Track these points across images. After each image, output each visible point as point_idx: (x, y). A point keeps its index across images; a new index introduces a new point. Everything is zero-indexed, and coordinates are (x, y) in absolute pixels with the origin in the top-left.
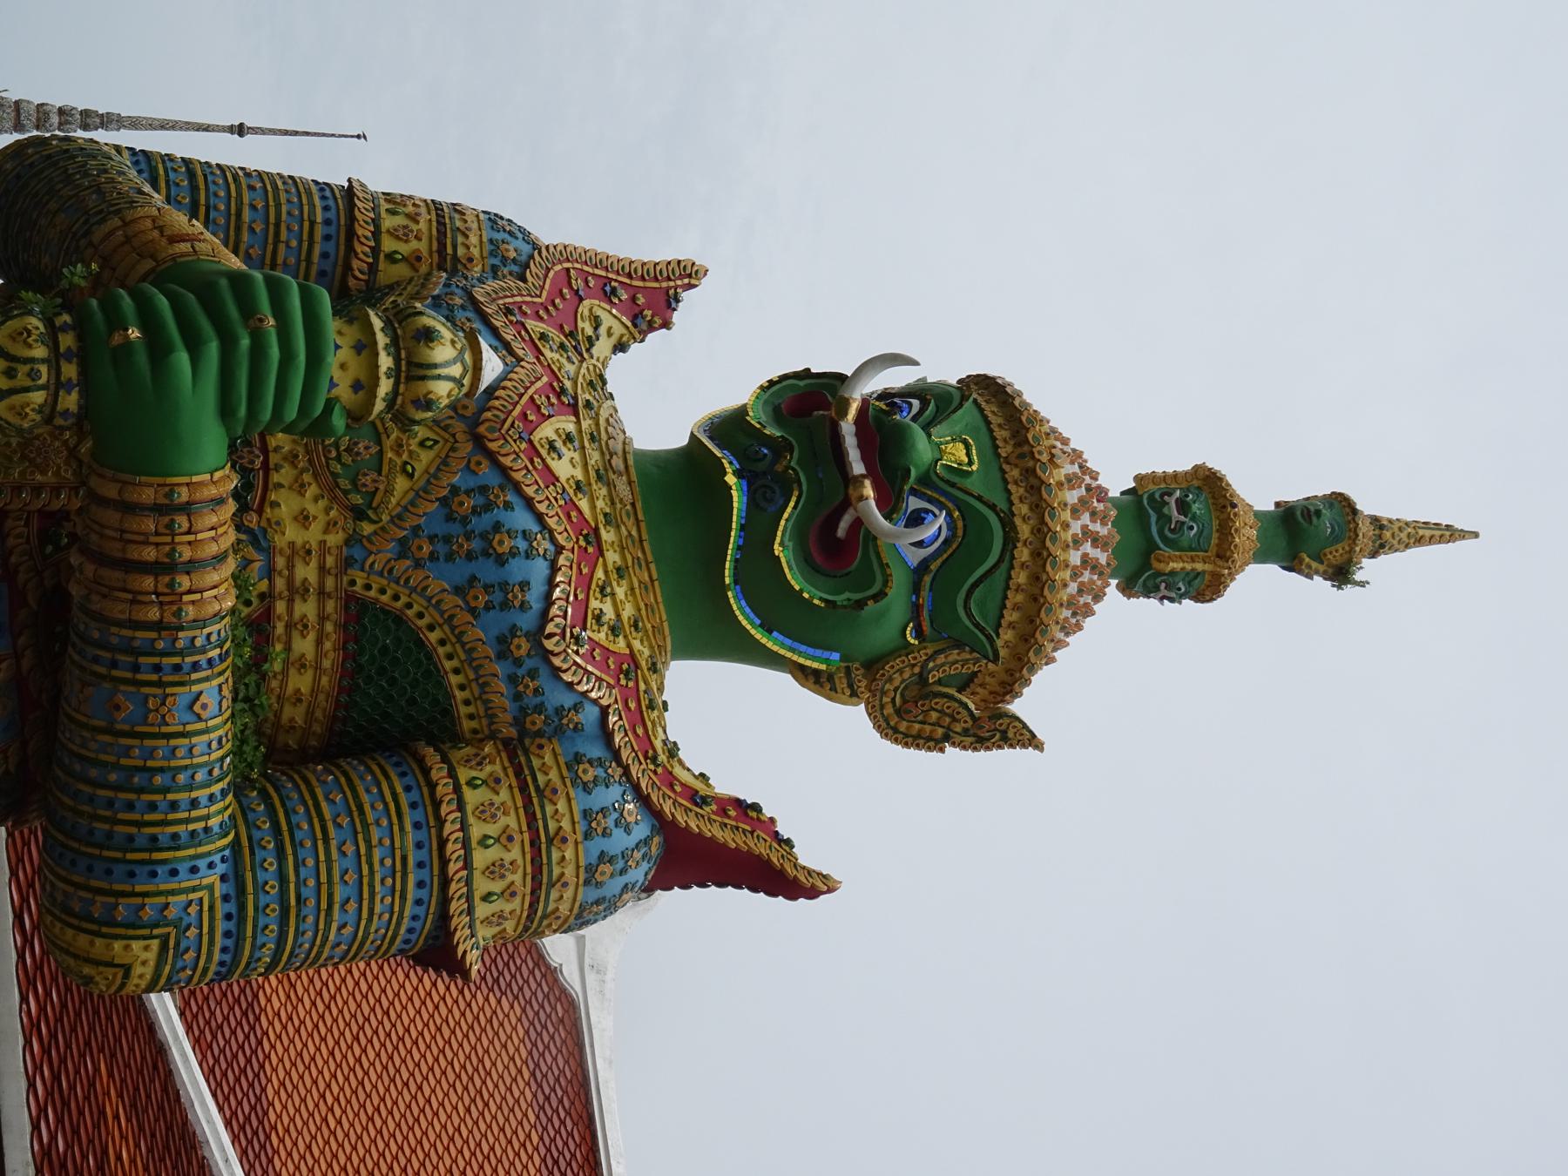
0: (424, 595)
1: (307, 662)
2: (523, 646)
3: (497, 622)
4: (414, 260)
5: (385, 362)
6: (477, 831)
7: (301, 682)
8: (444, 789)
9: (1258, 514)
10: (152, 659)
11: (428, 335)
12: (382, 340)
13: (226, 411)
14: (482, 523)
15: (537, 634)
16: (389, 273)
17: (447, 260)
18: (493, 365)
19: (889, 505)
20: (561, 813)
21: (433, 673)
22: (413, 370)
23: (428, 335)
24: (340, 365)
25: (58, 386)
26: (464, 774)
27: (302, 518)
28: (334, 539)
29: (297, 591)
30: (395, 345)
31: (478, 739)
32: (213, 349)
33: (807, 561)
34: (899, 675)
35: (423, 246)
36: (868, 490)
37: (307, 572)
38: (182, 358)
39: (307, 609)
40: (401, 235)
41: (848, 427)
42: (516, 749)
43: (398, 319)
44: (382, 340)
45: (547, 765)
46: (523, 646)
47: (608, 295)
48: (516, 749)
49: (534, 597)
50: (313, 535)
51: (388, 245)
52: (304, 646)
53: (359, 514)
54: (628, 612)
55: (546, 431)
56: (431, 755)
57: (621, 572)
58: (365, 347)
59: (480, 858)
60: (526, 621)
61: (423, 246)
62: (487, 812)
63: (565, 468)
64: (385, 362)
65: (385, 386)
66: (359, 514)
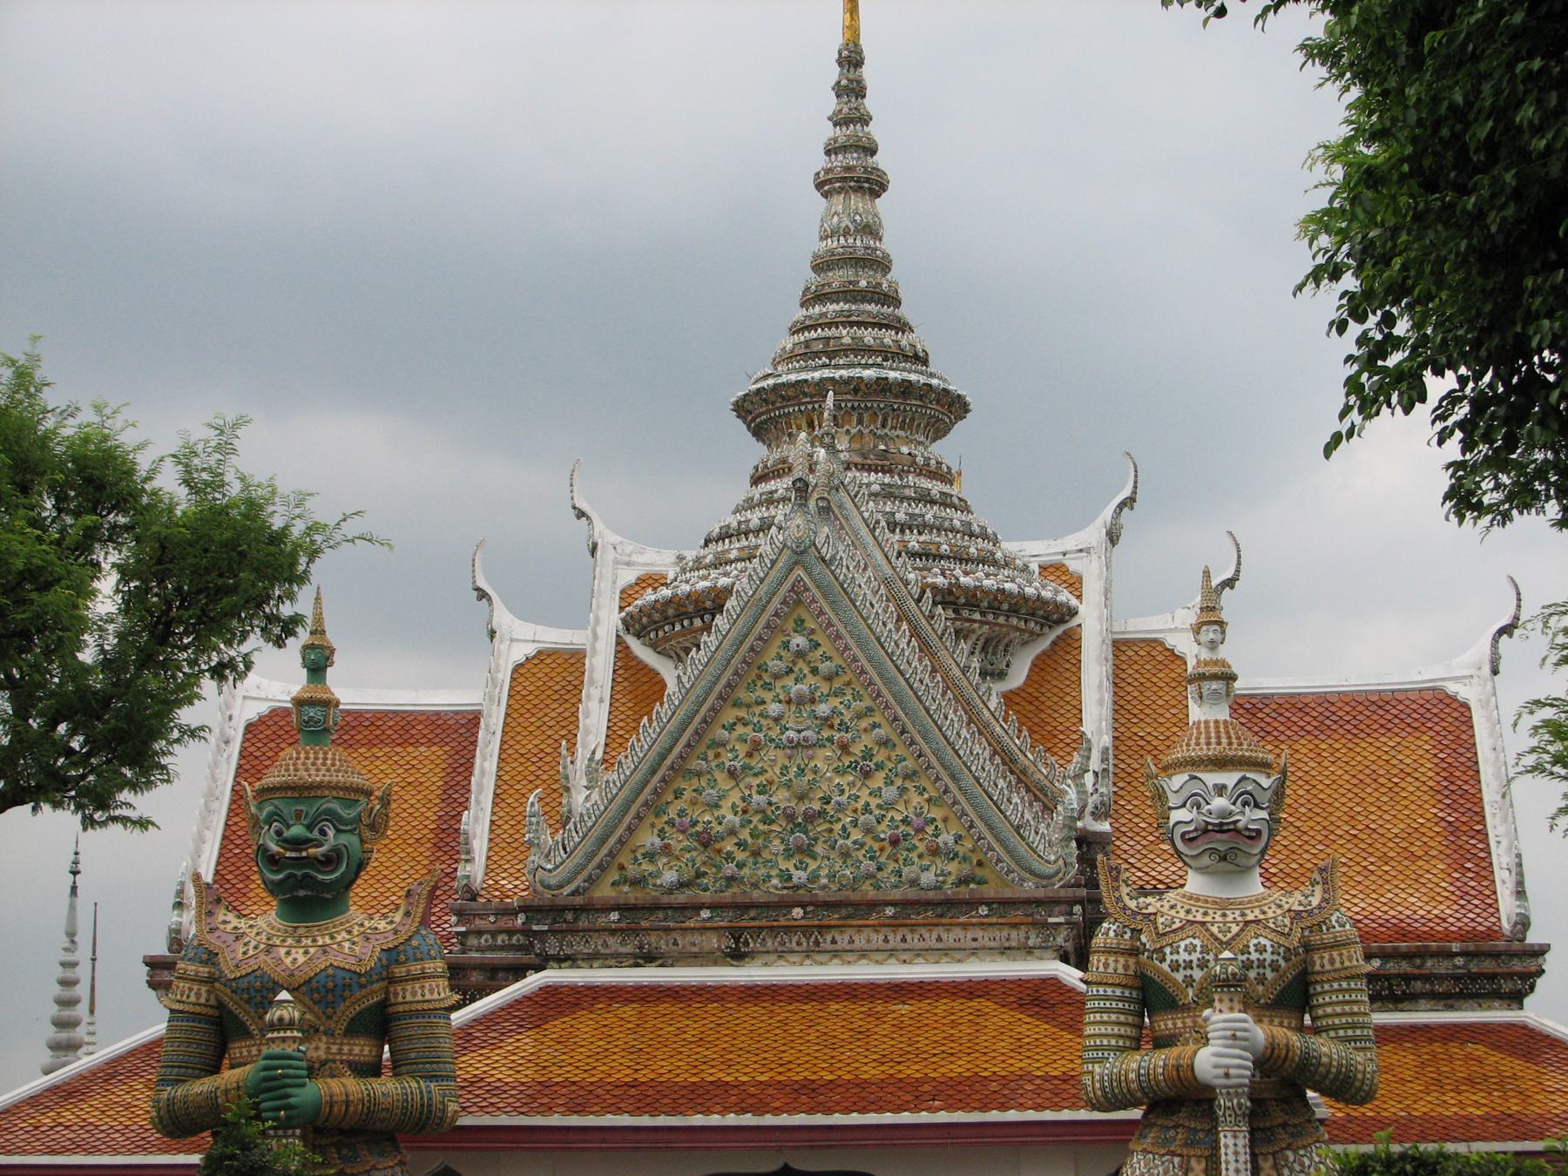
0: (347, 1010)
1: (361, 1049)
2: (363, 980)
3: (355, 987)
4: (208, 992)
5: (289, 1034)
6: (419, 998)
7: (366, 1052)
8: (407, 1007)
9: (310, 681)
10: (371, 1107)
11: (281, 1019)
12: (282, 1034)
13: (304, 1085)
14: (323, 991)
15: (360, 975)
16: (213, 1002)
17: (211, 980)
18: (284, 995)
19: (321, 845)
20: (416, 968)
21: (368, 1009)
22: (291, 1025)
23: (281, 1019)
24: (290, 1049)
25: (293, 1135)
26: (400, 999)
27: (318, 1049)
28: (324, 1039)
29: (340, 1052)
30: (285, 1030)
31: (387, 993)
32: (290, 1090)
33: (332, 872)
34: (367, 834)
35: (204, 989)
36: (312, 851)
37: (334, 1049)
38: (292, 1100)
39: (346, 1049)
40: (198, 995)
41: (288, 854)
42: (392, 980)
43: (272, 1027)
44: (282, 1034)
45: (400, 971)
46: (363, 980)
47: (210, 914)
48: (392, 980)
49: (348, 975)
50: (323, 1046)
51: (203, 1000)
52: (357, 1050)
53: (317, 1031)
54: (344, 934)
55: (288, 961)
56: (391, 1010)
57: (332, 938)
58: (284, 1040)
59: (428, 997)
60: (355, 977)
61: (204, 989)
62: (414, 994)
63: (301, 959)
64: (289, 1034)
65: (296, 1034)
66: (317, 1031)
